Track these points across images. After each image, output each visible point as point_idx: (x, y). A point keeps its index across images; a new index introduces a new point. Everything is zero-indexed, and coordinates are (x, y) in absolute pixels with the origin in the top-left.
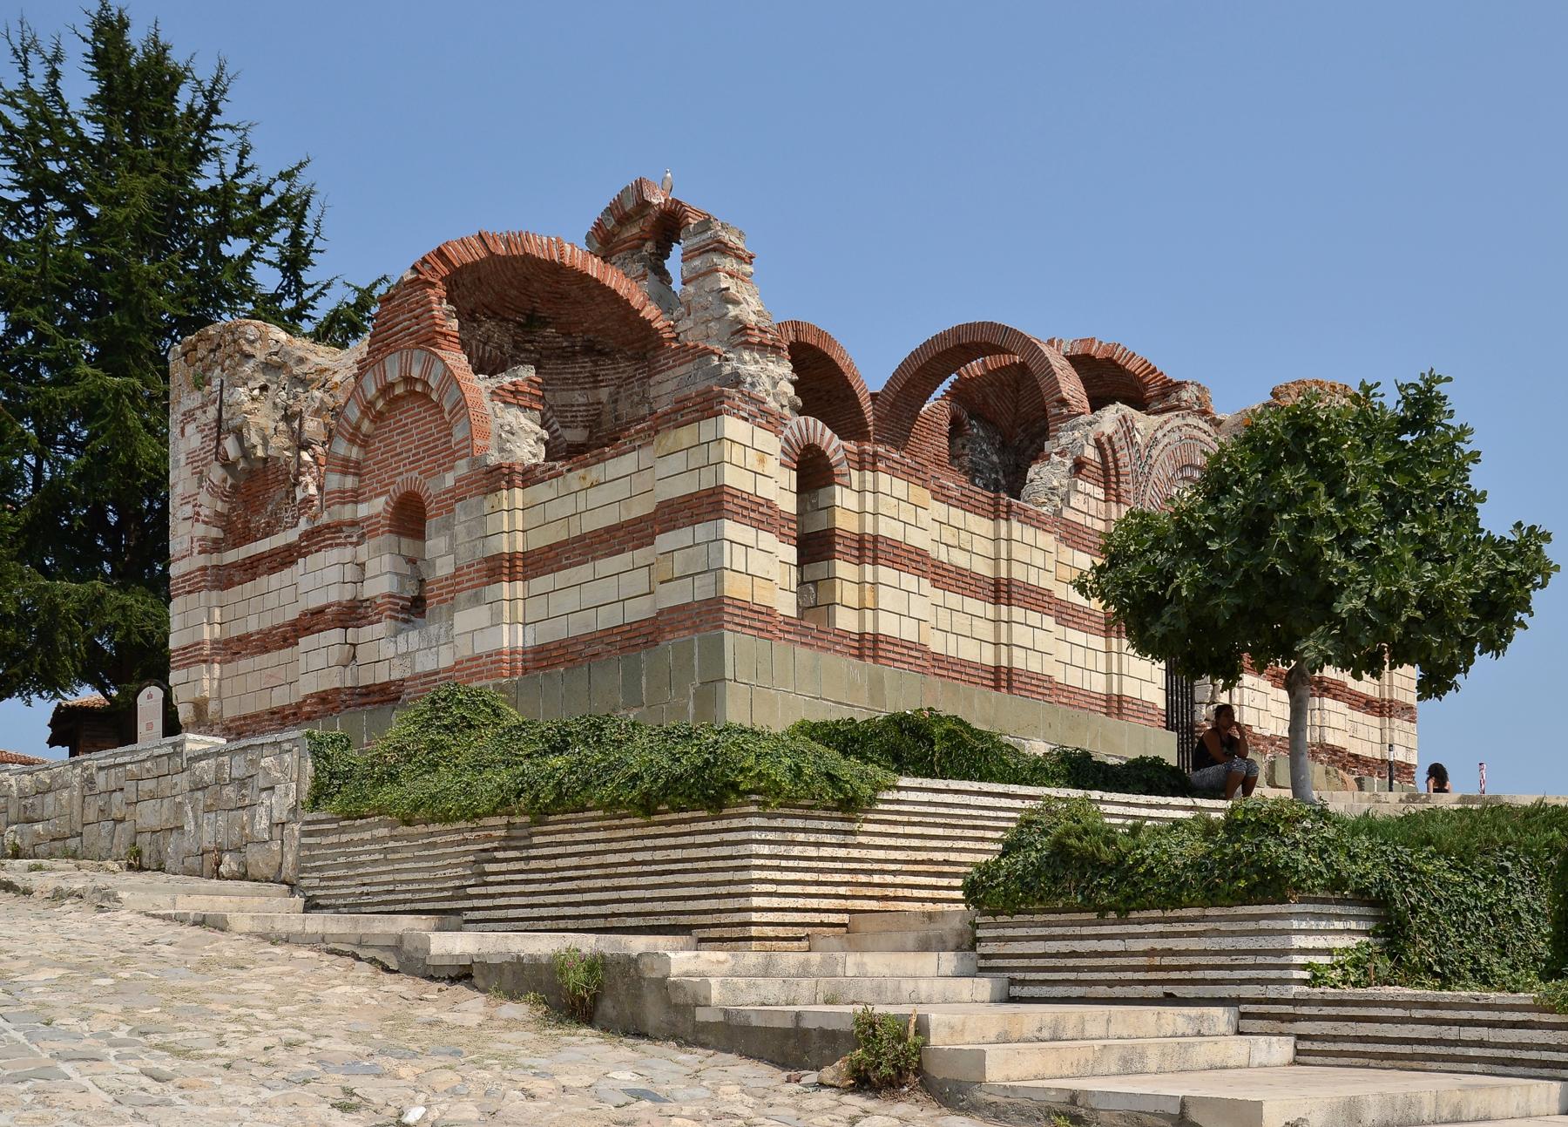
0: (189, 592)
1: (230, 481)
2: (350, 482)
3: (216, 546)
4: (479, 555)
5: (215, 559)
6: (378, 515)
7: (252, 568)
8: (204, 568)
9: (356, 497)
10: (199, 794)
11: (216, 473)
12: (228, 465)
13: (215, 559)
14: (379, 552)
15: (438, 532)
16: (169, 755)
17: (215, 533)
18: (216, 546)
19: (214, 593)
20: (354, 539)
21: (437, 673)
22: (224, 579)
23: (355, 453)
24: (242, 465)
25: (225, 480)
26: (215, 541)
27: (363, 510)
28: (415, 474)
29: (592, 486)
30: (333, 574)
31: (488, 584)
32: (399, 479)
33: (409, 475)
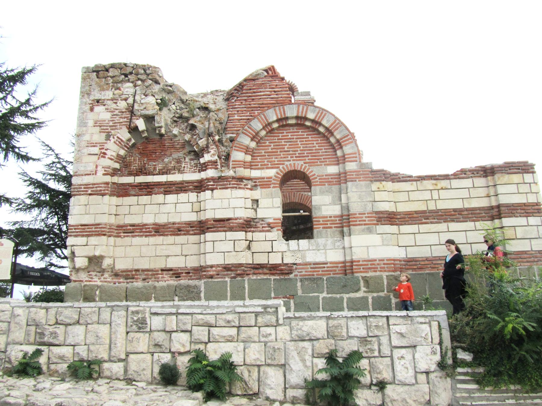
0: (90, 194)
1: (133, 141)
2: (249, 158)
3: (114, 172)
4: (369, 209)
5: (116, 179)
6: (271, 178)
7: (148, 189)
8: (107, 183)
9: (250, 166)
10: (307, 344)
11: (125, 135)
12: (133, 130)
13: (116, 179)
14: (272, 196)
15: (322, 193)
16: (257, 314)
17: (117, 166)
18: (114, 172)
19: (114, 198)
20: (249, 187)
21: (326, 263)
22: (122, 191)
23: (253, 145)
24: (146, 134)
25: (129, 140)
26: (115, 170)
27: (255, 173)
28: (302, 162)
29: (442, 189)
30: (241, 203)
31: (378, 225)
32: (286, 163)
33: (296, 162)
